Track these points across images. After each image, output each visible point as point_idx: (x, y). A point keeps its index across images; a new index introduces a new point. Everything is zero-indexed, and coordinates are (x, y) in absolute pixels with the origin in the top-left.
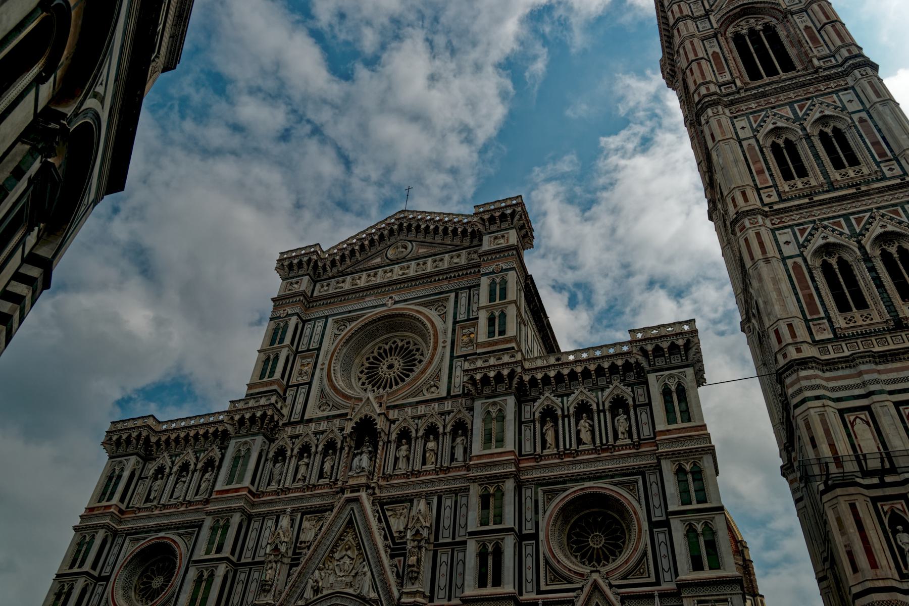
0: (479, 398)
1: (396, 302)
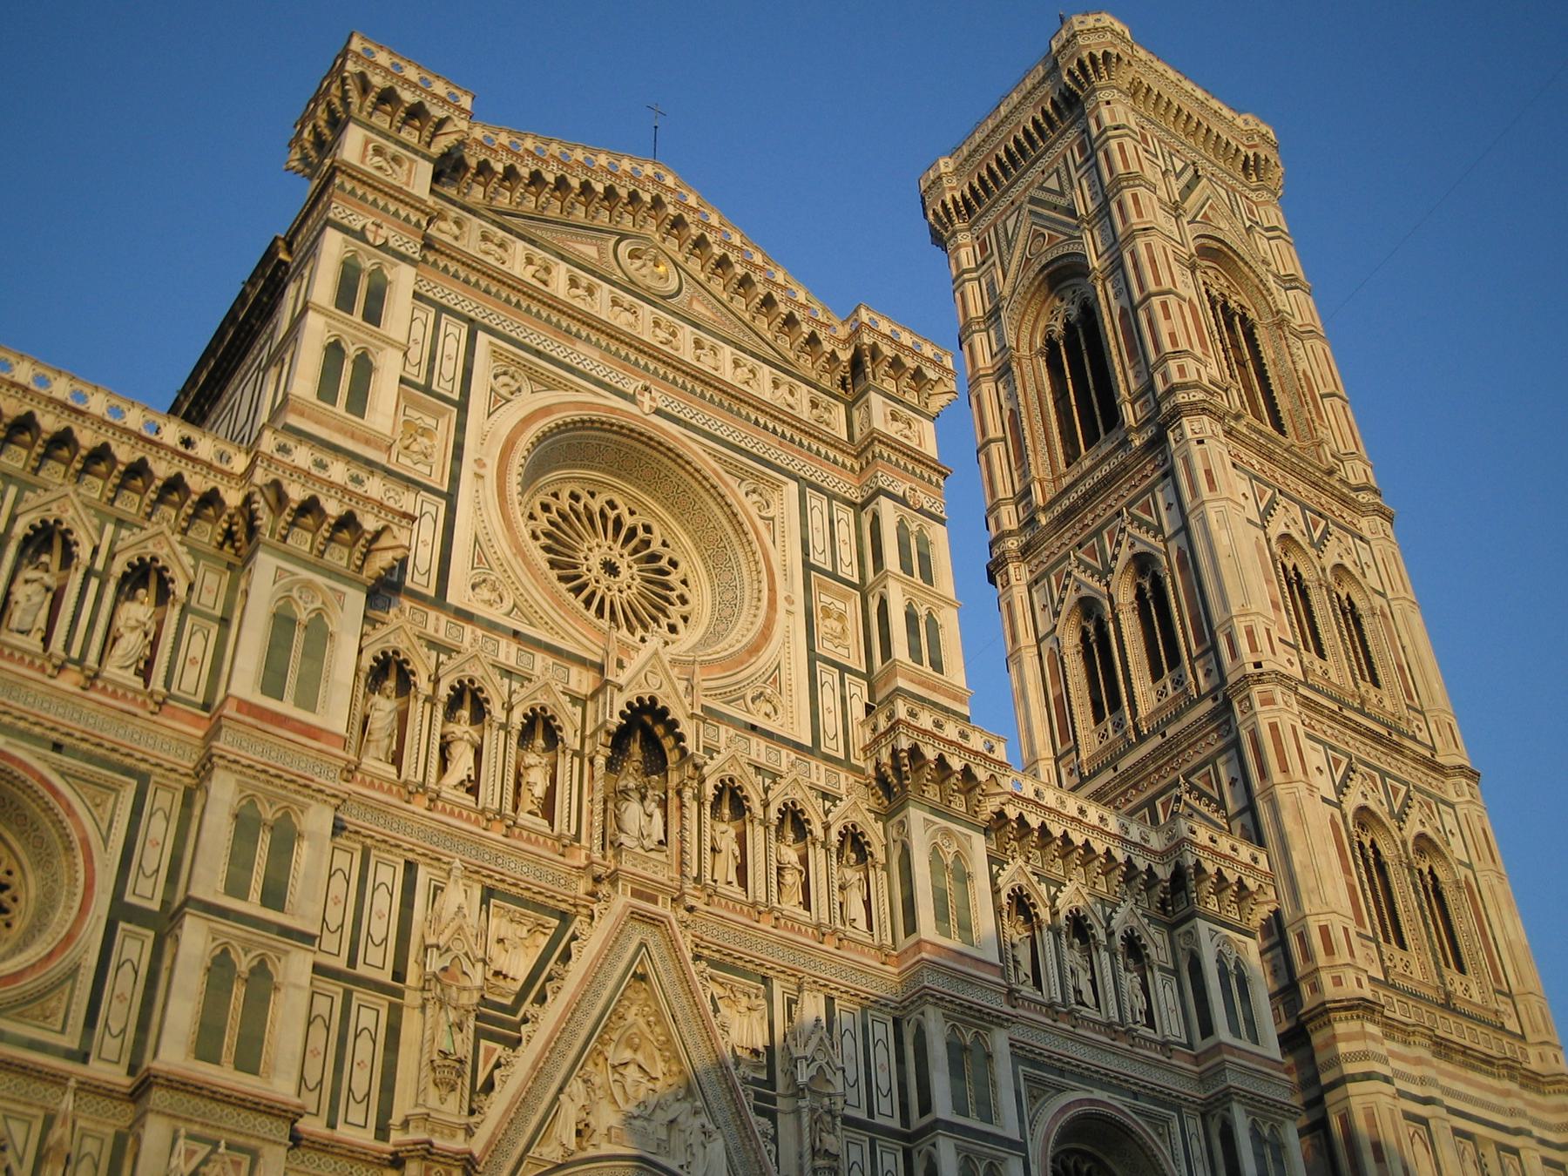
0: (921, 804)
1: (658, 412)
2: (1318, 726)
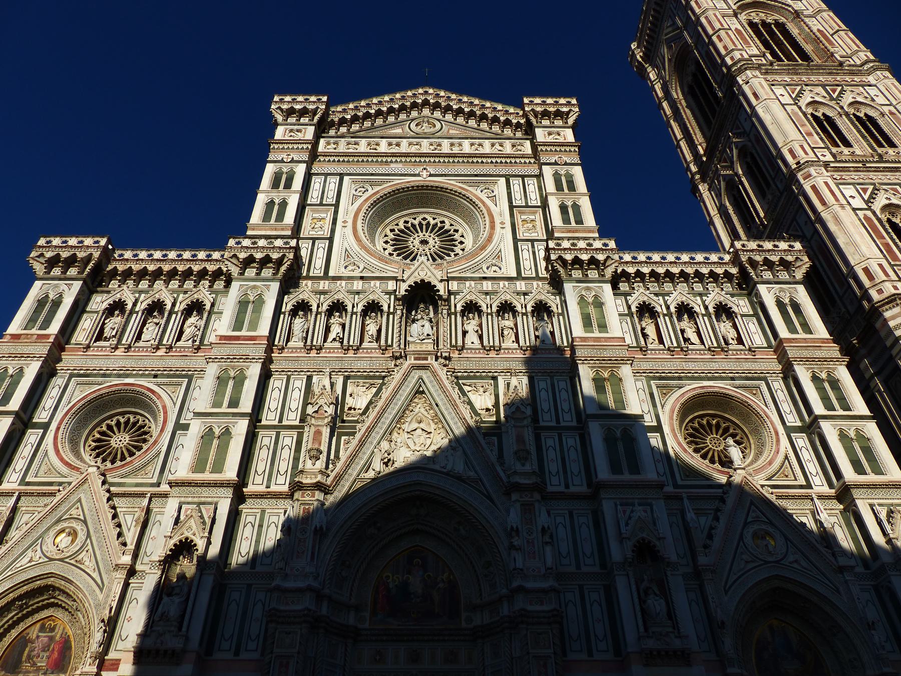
0: (570, 281)
1: (431, 175)
2: (847, 178)
